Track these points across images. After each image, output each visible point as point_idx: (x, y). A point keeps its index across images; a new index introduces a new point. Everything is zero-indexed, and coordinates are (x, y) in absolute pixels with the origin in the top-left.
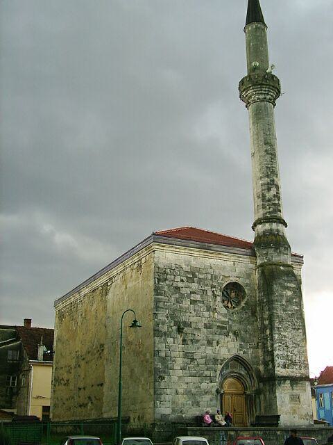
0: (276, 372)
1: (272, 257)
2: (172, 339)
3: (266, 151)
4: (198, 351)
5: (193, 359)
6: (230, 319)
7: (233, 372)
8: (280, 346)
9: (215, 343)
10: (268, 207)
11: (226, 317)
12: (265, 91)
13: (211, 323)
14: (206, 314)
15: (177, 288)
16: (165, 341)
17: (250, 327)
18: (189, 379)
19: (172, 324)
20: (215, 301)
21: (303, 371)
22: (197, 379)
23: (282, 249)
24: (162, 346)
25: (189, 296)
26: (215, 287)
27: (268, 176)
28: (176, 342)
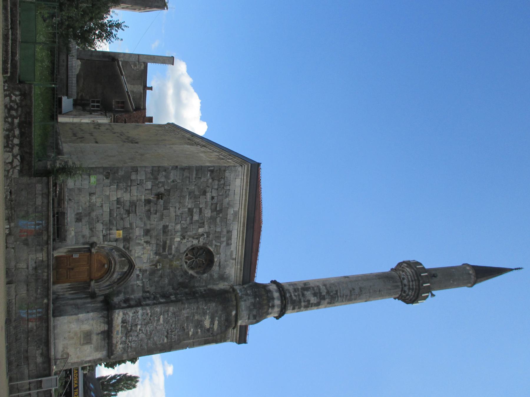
0: (117, 311)
1: (245, 301)
2: (150, 187)
3: (354, 289)
4: (138, 219)
5: (128, 212)
6: (174, 256)
7: (115, 264)
8: (148, 314)
9: (148, 238)
10: (296, 294)
11: (176, 251)
13: (170, 233)
14: (178, 227)
15: (204, 193)
16: (147, 179)
17: (167, 281)
18: (106, 209)
19: (166, 187)
20: (193, 238)
22: (106, 218)
23: (254, 312)
24: (141, 176)
25: (197, 206)
26: (208, 237)
27: (328, 293)
28: (147, 192)
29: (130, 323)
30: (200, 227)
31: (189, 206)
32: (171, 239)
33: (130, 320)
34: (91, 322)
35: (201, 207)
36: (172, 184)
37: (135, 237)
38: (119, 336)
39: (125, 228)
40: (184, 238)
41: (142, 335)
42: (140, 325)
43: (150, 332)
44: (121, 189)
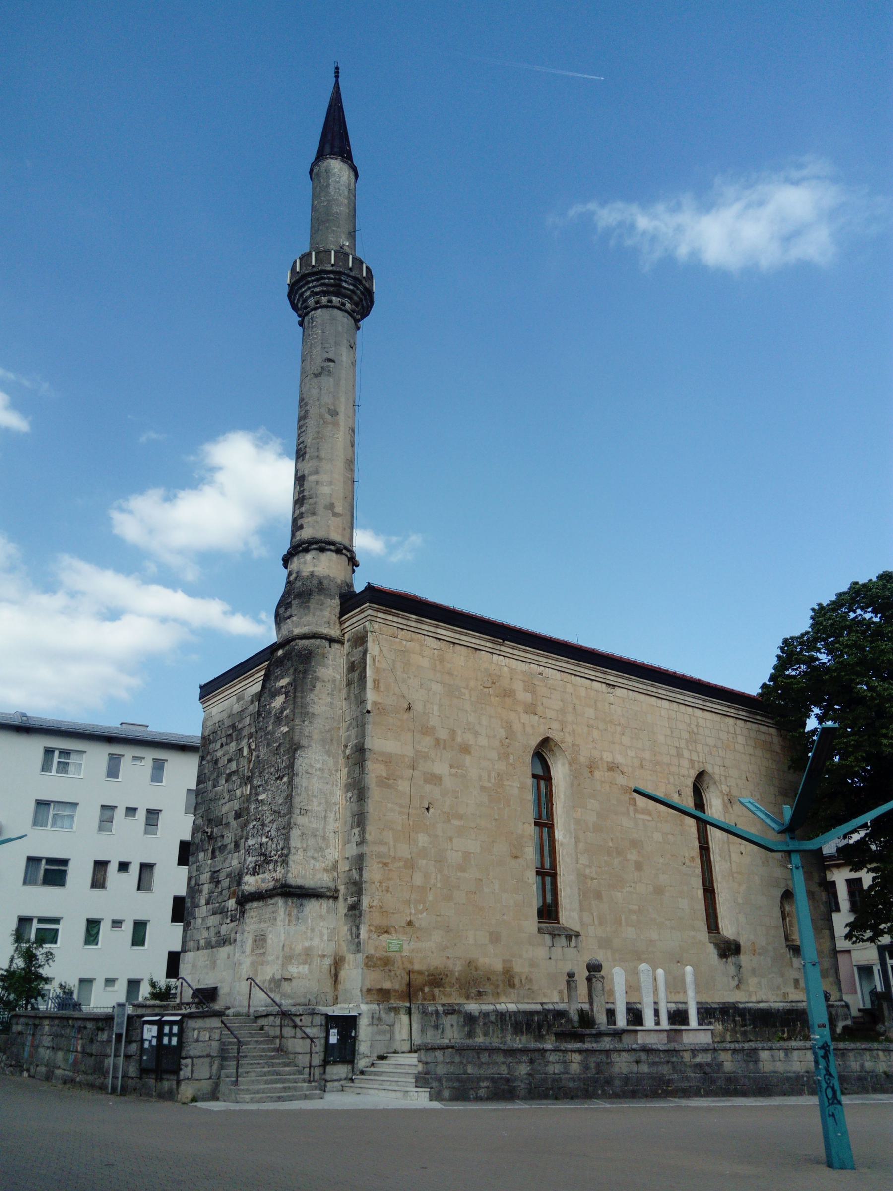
8: (254, 826)
12: (298, 300)
33: (255, 858)
34: (245, 934)
35: (226, 762)
36: (205, 818)
37: (239, 865)
38: (268, 877)
41: (273, 833)
42: (262, 838)
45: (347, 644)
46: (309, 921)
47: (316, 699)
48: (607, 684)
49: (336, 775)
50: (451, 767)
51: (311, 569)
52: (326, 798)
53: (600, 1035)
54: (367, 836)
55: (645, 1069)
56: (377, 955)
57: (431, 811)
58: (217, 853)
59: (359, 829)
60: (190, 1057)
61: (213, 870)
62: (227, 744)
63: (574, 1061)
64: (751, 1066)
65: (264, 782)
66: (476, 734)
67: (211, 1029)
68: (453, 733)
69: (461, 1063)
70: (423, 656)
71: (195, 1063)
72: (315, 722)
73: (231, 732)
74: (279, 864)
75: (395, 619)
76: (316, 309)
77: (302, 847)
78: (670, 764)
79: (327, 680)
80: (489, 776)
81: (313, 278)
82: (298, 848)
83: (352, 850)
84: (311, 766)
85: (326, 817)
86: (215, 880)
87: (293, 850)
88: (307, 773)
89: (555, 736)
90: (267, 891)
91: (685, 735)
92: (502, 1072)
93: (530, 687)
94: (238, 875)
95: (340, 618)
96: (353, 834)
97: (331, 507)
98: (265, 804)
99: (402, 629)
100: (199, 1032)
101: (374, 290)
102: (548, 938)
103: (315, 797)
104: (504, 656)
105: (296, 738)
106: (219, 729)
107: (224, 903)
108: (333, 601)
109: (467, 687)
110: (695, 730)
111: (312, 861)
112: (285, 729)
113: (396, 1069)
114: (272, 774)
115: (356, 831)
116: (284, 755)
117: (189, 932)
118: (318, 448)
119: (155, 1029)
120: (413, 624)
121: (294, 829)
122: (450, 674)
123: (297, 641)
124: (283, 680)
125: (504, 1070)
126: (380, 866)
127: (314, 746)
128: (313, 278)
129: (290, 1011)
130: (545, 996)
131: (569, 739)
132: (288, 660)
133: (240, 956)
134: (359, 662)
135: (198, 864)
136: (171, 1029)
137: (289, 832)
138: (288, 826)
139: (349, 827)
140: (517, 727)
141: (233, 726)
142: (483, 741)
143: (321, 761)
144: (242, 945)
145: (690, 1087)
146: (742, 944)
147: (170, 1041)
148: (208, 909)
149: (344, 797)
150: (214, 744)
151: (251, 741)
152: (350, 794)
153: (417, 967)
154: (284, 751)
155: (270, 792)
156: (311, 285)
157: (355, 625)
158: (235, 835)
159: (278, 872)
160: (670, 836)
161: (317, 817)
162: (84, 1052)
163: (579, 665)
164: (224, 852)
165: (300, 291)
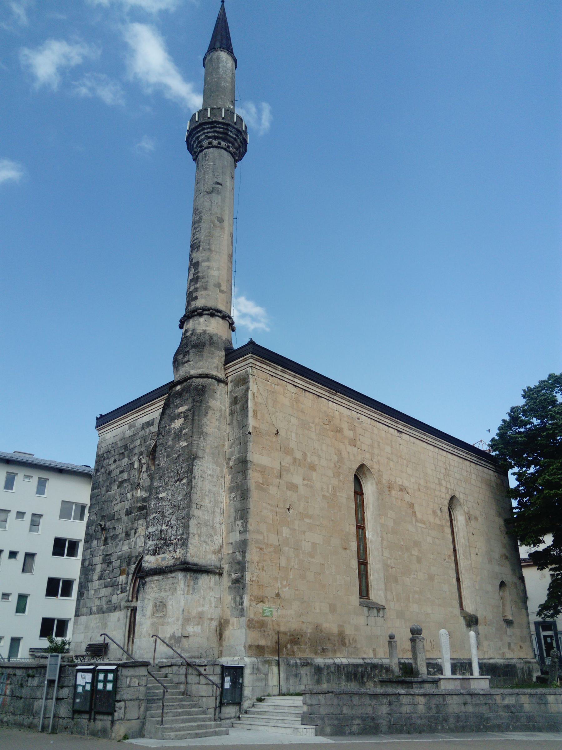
5: (110, 563)
8: (154, 518)
12: (195, 142)
21: (179, 553)
29: (158, 542)
30: (134, 468)
31: (116, 488)
32: (137, 502)
34: (146, 601)
35: (118, 473)
36: (98, 515)
38: (168, 557)
39: (120, 565)
40: (139, 484)
41: (173, 522)
42: (162, 527)
43: (172, 508)
44: (93, 576)
45: (230, 385)
46: (202, 591)
47: (208, 423)
48: (398, 431)
49: (221, 481)
50: (304, 479)
51: (204, 328)
52: (214, 497)
53: (423, 682)
54: (249, 526)
55: (470, 709)
56: (256, 619)
57: (291, 511)
58: (109, 541)
59: (242, 521)
60: (123, 700)
61: (105, 554)
62: (119, 460)
63: (420, 703)
64: (543, 707)
65: (164, 484)
66: (319, 457)
67: (139, 677)
68: (305, 454)
69: (339, 705)
70: (285, 397)
71: (127, 706)
72: (208, 439)
73: (123, 451)
74: (179, 546)
75: (268, 368)
76: (208, 148)
77: (197, 534)
78: (435, 490)
79: (216, 409)
80: (328, 488)
81: (208, 126)
82: (195, 534)
83: (236, 537)
84: (204, 472)
85: (214, 512)
86: (107, 561)
87: (191, 536)
88: (202, 477)
89: (368, 463)
90: (166, 567)
91: (443, 471)
92: (369, 712)
93: (352, 428)
94: (128, 557)
95: (225, 365)
96: (236, 525)
97: (219, 285)
98: (165, 501)
99: (272, 376)
100: (131, 679)
101: (248, 142)
102: (365, 609)
103: (207, 495)
104: (336, 403)
105: (194, 450)
106: (112, 449)
107: (115, 579)
108: (220, 352)
109: (313, 423)
110: (448, 468)
111: (205, 545)
112: (184, 444)
113: (276, 709)
114: (171, 477)
115: (240, 522)
116: (183, 463)
117: (82, 601)
118: (209, 243)
119: (89, 677)
120: (280, 373)
121: (192, 519)
122: (303, 412)
123: (194, 379)
124: (182, 408)
125: (369, 710)
126: (258, 550)
127: (206, 457)
128: (208, 126)
129: (195, 662)
130: (365, 653)
131: (376, 466)
132: (187, 392)
133: (140, 618)
134: (241, 397)
135: (91, 549)
136: (106, 677)
137: (188, 521)
138: (188, 517)
139: (232, 519)
140: (344, 454)
141: (126, 447)
142: (324, 463)
143: (211, 469)
144: (143, 610)
145: (502, 723)
146: (479, 617)
147: (105, 686)
148: (100, 583)
149: (228, 497)
150: (108, 460)
151: (141, 457)
152: (233, 495)
153: (282, 629)
154: (183, 460)
155: (169, 491)
156: (206, 131)
157: (238, 370)
158: (126, 527)
159: (178, 552)
160: (436, 540)
161: (208, 511)
162: (12, 695)
163: (381, 415)
164: (115, 540)
165: (197, 135)
